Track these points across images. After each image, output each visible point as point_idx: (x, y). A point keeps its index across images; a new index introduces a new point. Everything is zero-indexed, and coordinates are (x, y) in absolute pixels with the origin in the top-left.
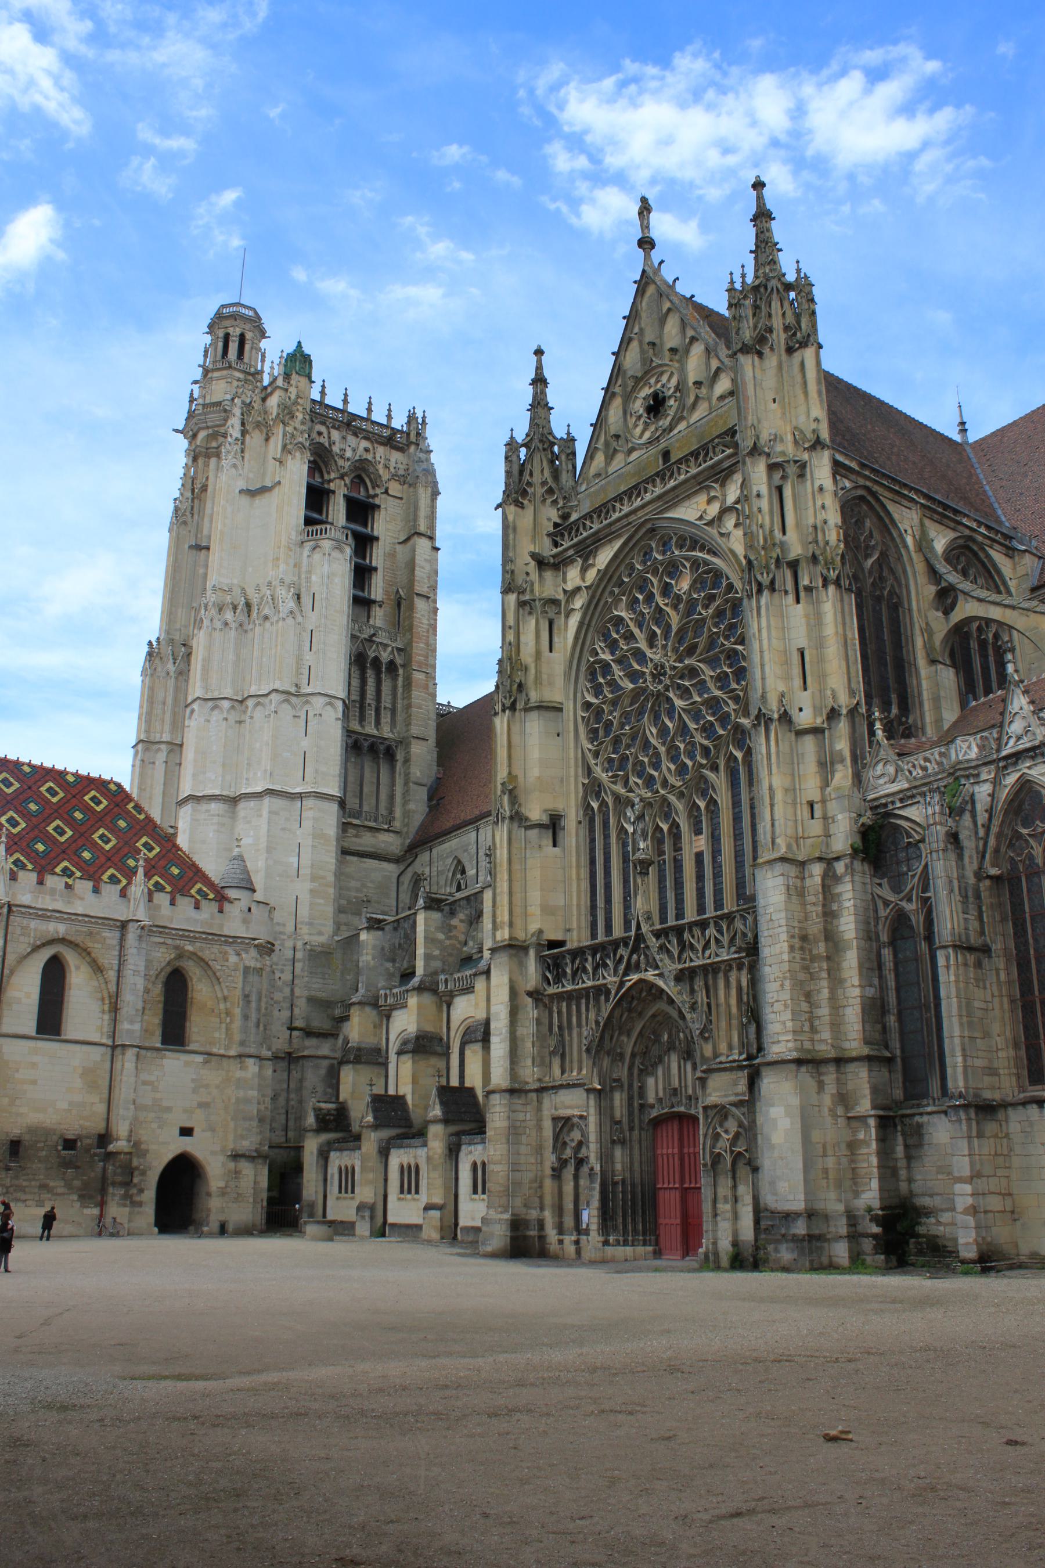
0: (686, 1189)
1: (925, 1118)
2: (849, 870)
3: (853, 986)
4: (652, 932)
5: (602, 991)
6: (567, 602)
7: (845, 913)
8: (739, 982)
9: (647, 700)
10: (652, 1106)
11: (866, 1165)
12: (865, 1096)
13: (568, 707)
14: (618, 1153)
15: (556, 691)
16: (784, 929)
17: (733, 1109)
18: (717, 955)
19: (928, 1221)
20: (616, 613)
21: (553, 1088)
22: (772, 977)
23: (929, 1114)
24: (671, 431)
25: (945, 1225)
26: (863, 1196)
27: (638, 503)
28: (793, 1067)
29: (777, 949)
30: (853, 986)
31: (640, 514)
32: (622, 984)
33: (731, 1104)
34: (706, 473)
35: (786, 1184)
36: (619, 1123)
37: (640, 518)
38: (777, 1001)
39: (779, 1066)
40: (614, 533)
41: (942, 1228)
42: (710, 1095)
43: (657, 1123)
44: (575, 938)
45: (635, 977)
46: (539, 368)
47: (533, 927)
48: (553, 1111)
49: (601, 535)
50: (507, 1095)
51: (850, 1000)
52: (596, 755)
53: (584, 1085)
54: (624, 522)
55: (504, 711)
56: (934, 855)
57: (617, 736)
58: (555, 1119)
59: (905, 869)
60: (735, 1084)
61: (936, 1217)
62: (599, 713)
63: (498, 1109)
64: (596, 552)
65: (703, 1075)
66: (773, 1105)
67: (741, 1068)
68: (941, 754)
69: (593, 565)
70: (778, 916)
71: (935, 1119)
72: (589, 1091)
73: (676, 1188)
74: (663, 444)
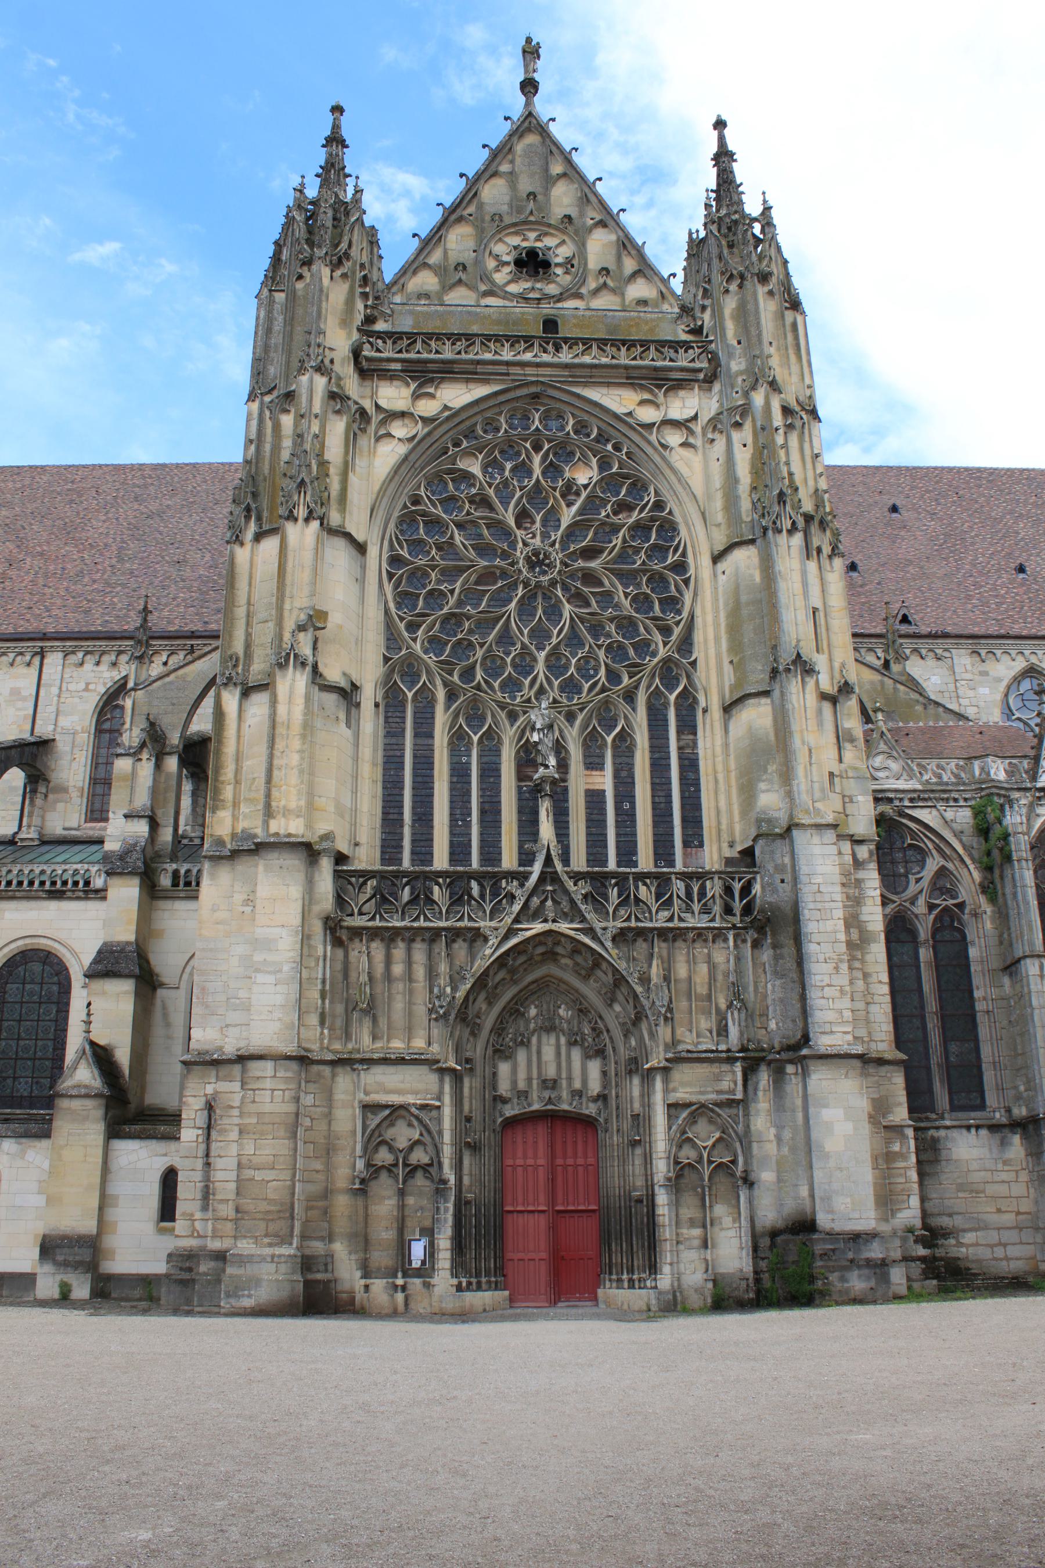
0: (559, 1212)
1: (942, 1133)
2: (875, 858)
3: (880, 982)
4: (567, 873)
5: (476, 937)
6: (383, 422)
7: (869, 902)
8: (709, 960)
9: (513, 586)
10: (505, 1101)
11: (903, 1180)
12: (900, 1104)
13: (373, 551)
14: (466, 1162)
15: (358, 524)
16: (840, 905)
17: (717, 1109)
18: (681, 919)
19: (946, 1242)
20: (461, 464)
21: (362, 1061)
22: (821, 958)
23: (947, 1128)
24: (559, 301)
25: (967, 1246)
26: (899, 1215)
27: (528, 356)
28: (857, 1063)
29: (829, 926)
30: (880, 982)
31: (529, 371)
32: (510, 933)
33: (716, 1104)
34: (644, 371)
35: (848, 1200)
36: (468, 1119)
37: (525, 375)
38: (828, 985)
39: (835, 1061)
40: (476, 373)
41: (964, 1250)
42: (674, 1090)
43: (511, 1123)
44: (364, 858)
45: (538, 927)
46: (336, 127)
47: (323, 827)
48: (362, 1096)
49: (457, 367)
50: (294, 1065)
51: (876, 997)
52: (412, 627)
53: (438, 1061)
54: (503, 369)
55: (307, 520)
56: (1024, 863)
57: (453, 615)
58: (369, 1108)
59: (902, 871)
60: (718, 1079)
61: (957, 1238)
62: (418, 575)
63: (268, 1084)
64: (439, 383)
65: (667, 1064)
66: (826, 1106)
67: (731, 1060)
68: (938, 766)
69: (432, 396)
70: (830, 889)
71: (955, 1134)
72: (442, 1071)
73: (593, 1211)
74: (547, 309)
